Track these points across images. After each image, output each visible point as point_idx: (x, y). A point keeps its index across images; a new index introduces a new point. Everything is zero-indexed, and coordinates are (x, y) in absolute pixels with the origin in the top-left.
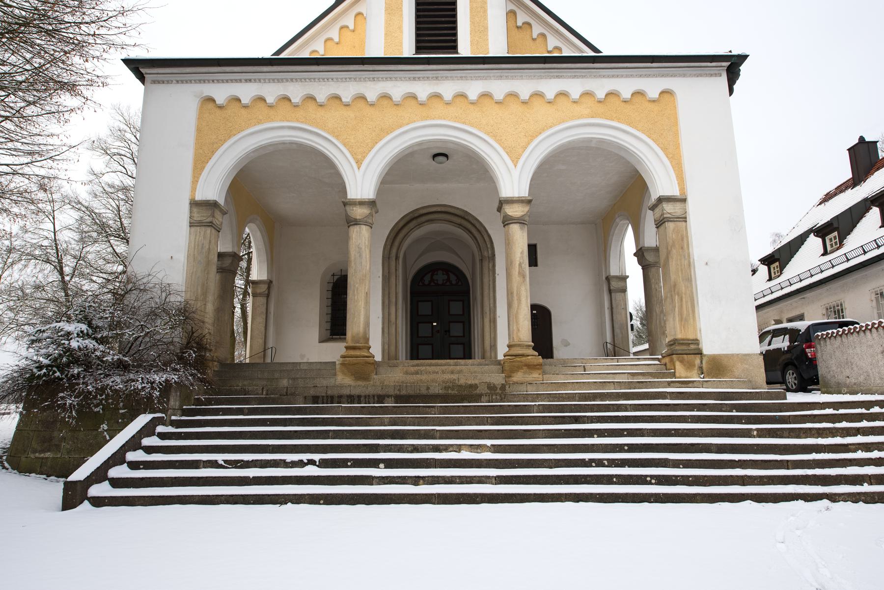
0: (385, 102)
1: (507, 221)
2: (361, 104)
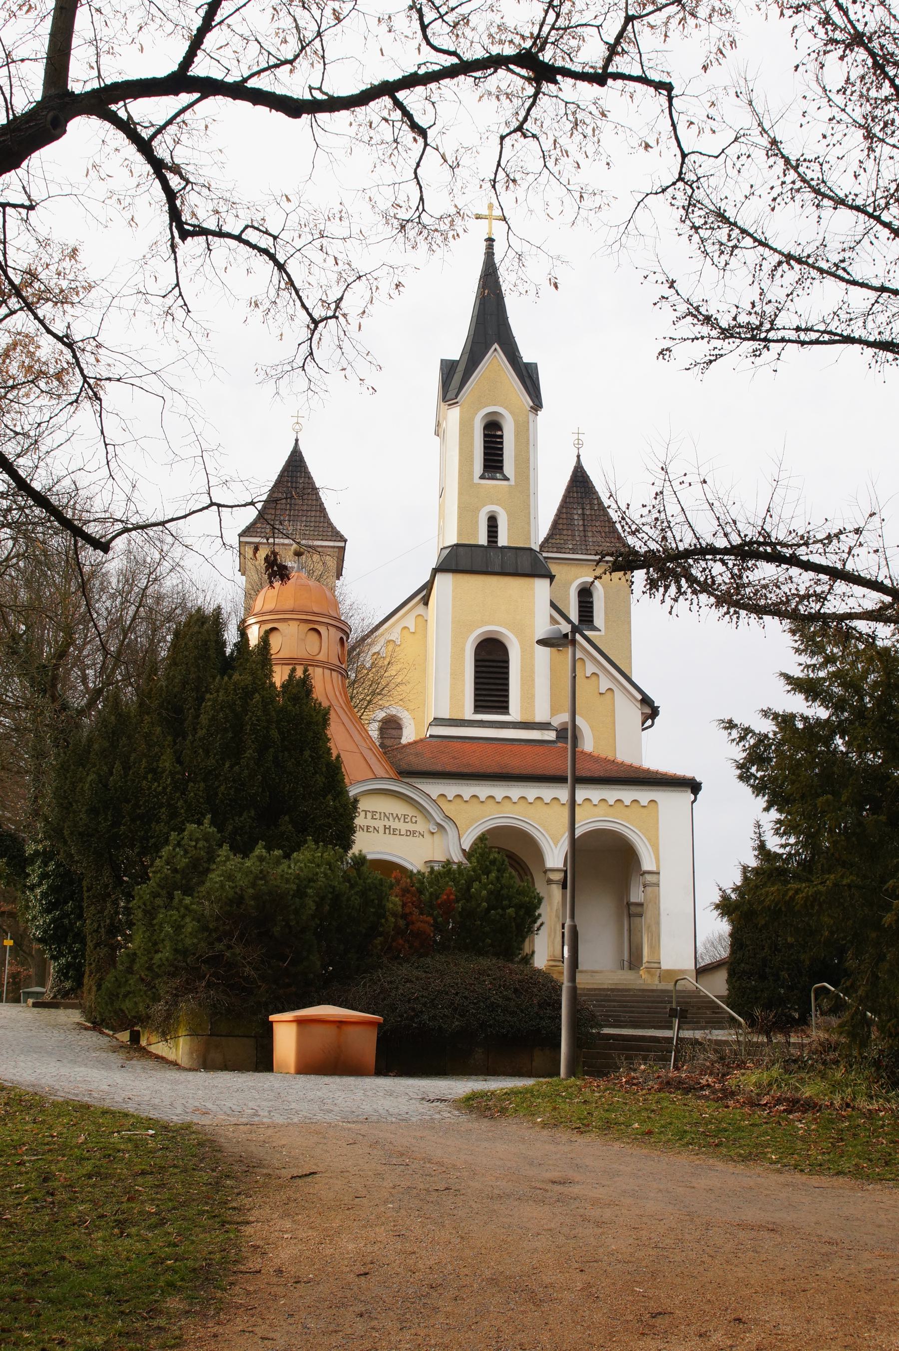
0: (475, 800)
1: (550, 882)
2: (458, 800)
